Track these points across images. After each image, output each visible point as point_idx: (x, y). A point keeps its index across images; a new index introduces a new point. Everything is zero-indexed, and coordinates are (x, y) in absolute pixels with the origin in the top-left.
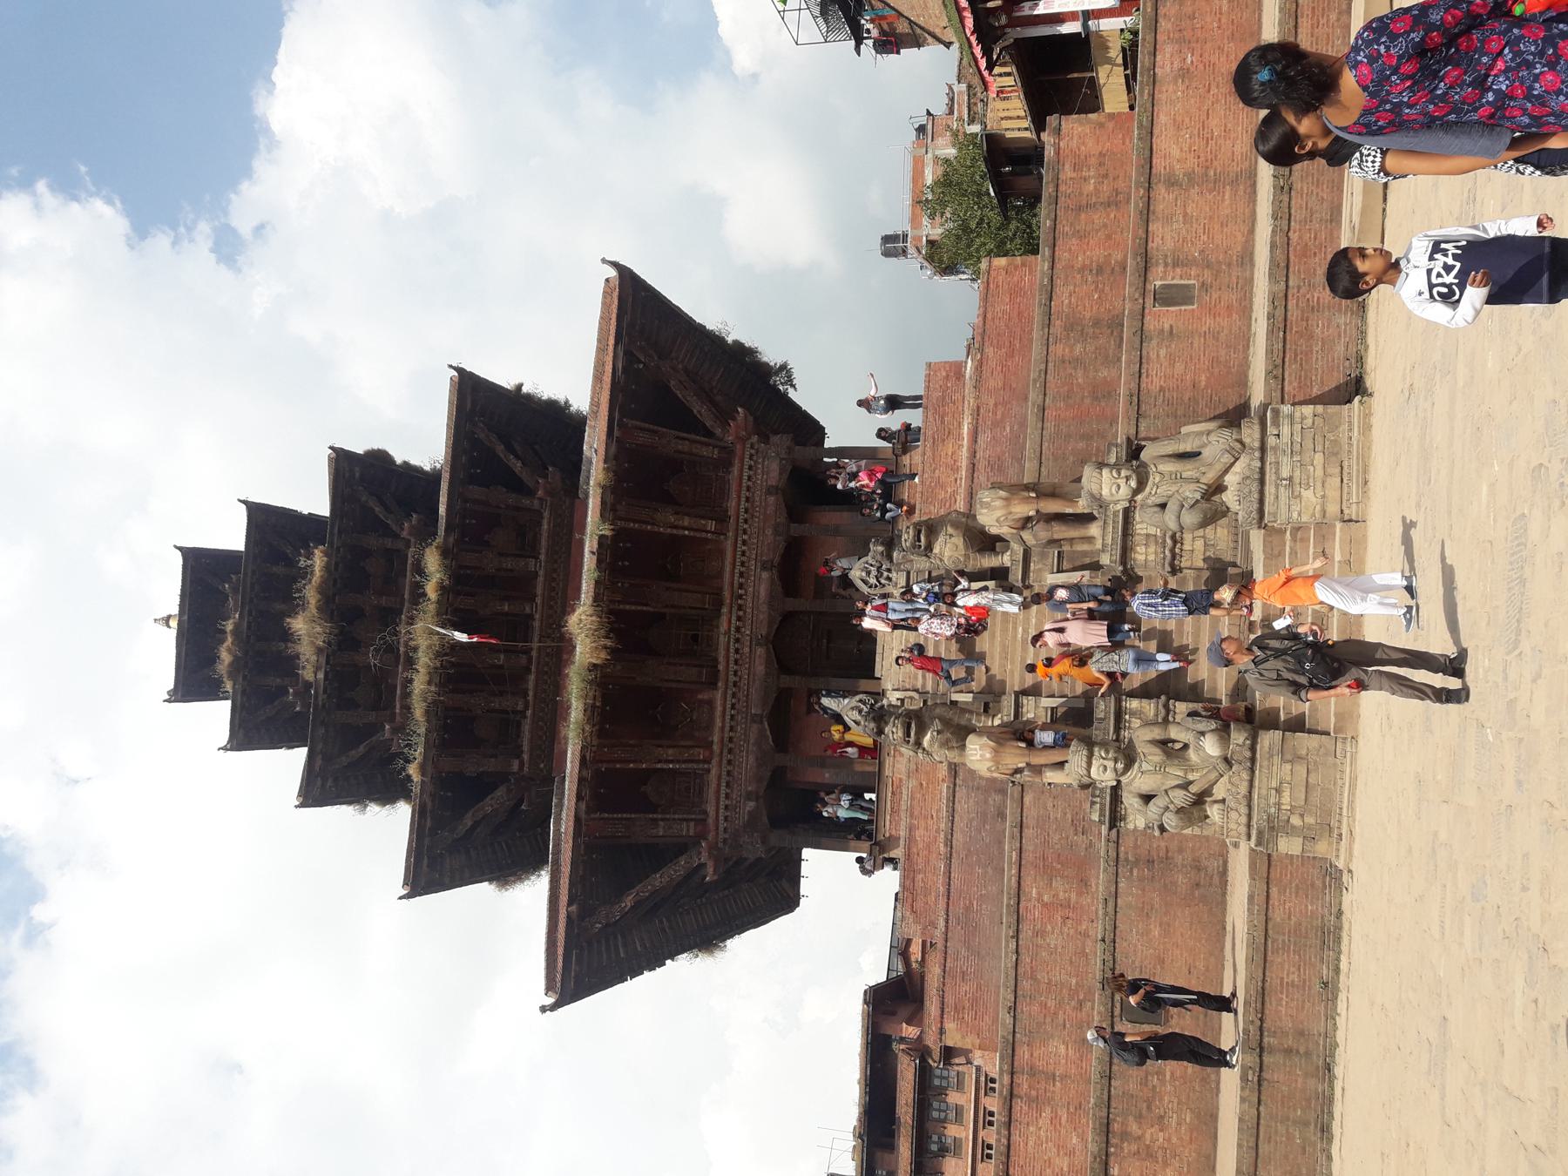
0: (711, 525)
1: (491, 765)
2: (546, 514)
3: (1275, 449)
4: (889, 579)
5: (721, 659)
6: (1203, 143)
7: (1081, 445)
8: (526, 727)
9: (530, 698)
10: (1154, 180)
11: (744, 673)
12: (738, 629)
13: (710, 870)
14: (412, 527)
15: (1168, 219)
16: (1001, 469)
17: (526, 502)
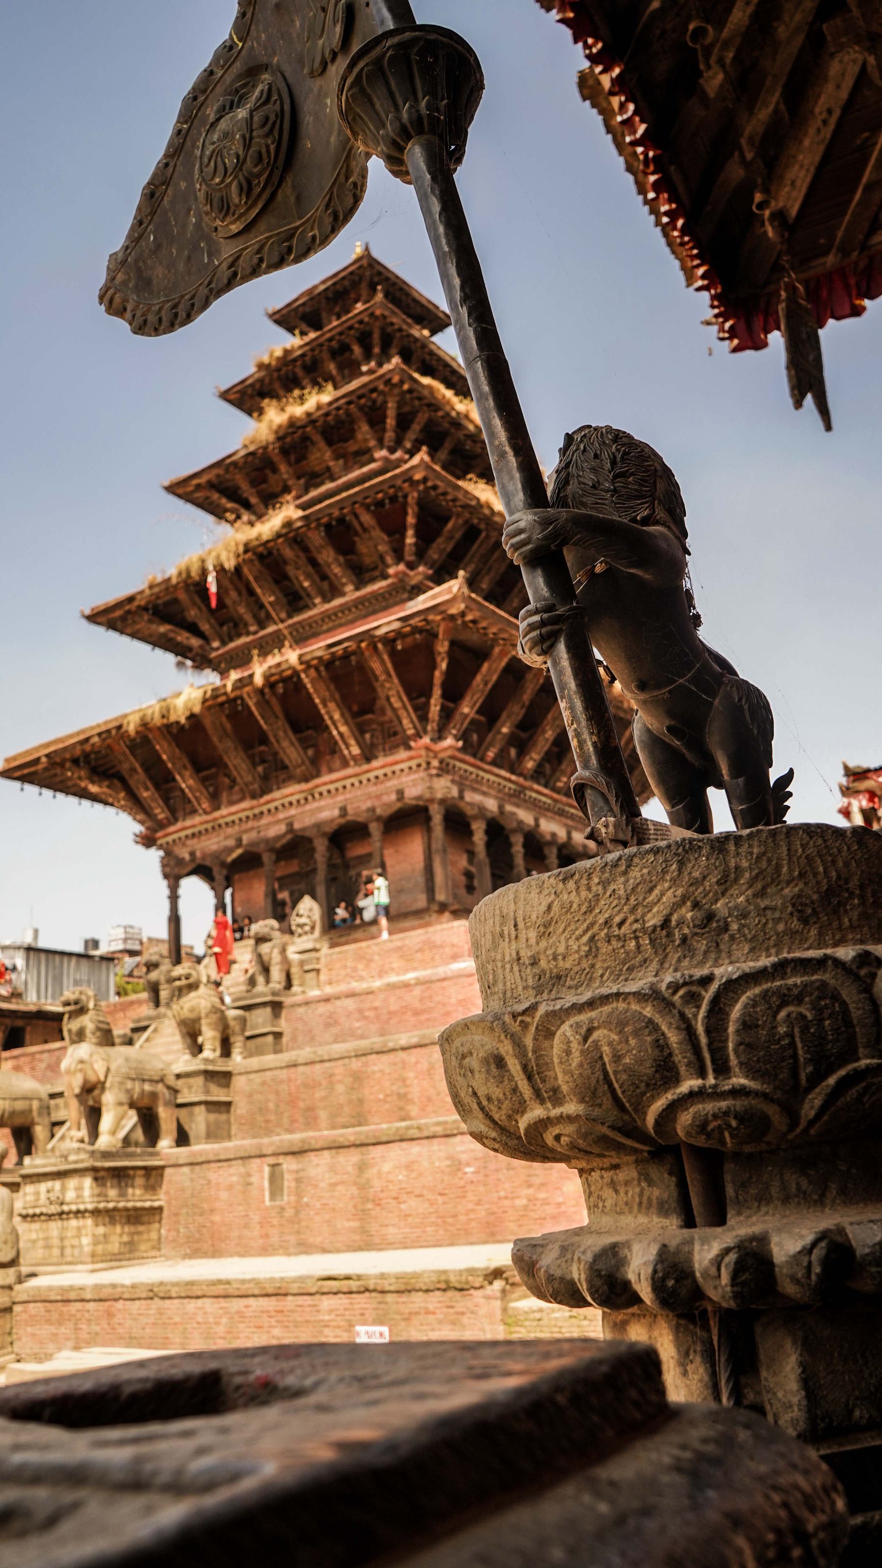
0: (356, 750)
1: (205, 627)
6: (394, 1194)
7: (271, 1105)
9: (262, 633)
10: (363, 1149)
11: (264, 821)
12: (291, 804)
15: (332, 1169)
16: (328, 1025)
17: (389, 560)
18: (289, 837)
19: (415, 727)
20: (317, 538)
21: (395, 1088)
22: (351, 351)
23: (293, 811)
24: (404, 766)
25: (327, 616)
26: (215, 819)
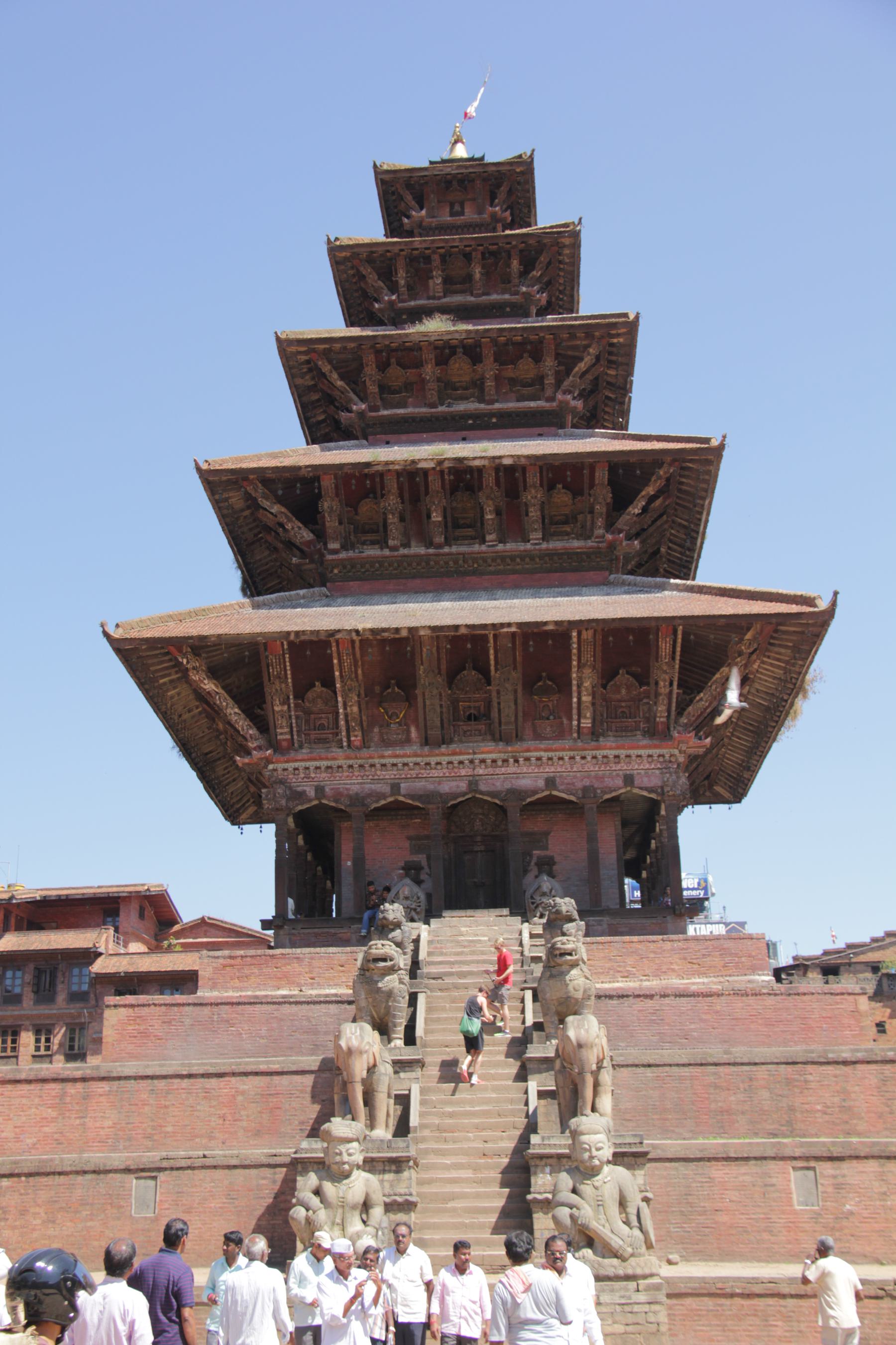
0: (586, 723)
1: (331, 523)
2: (590, 543)
3: (627, 1290)
4: (542, 916)
5: (453, 746)
8: (372, 552)
9: (403, 551)
12: (483, 761)
13: (246, 760)
14: (568, 403)
18: (469, 796)
19: (668, 717)
20: (533, 478)
21: (836, 1100)
22: (509, 266)
25: (502, 558)
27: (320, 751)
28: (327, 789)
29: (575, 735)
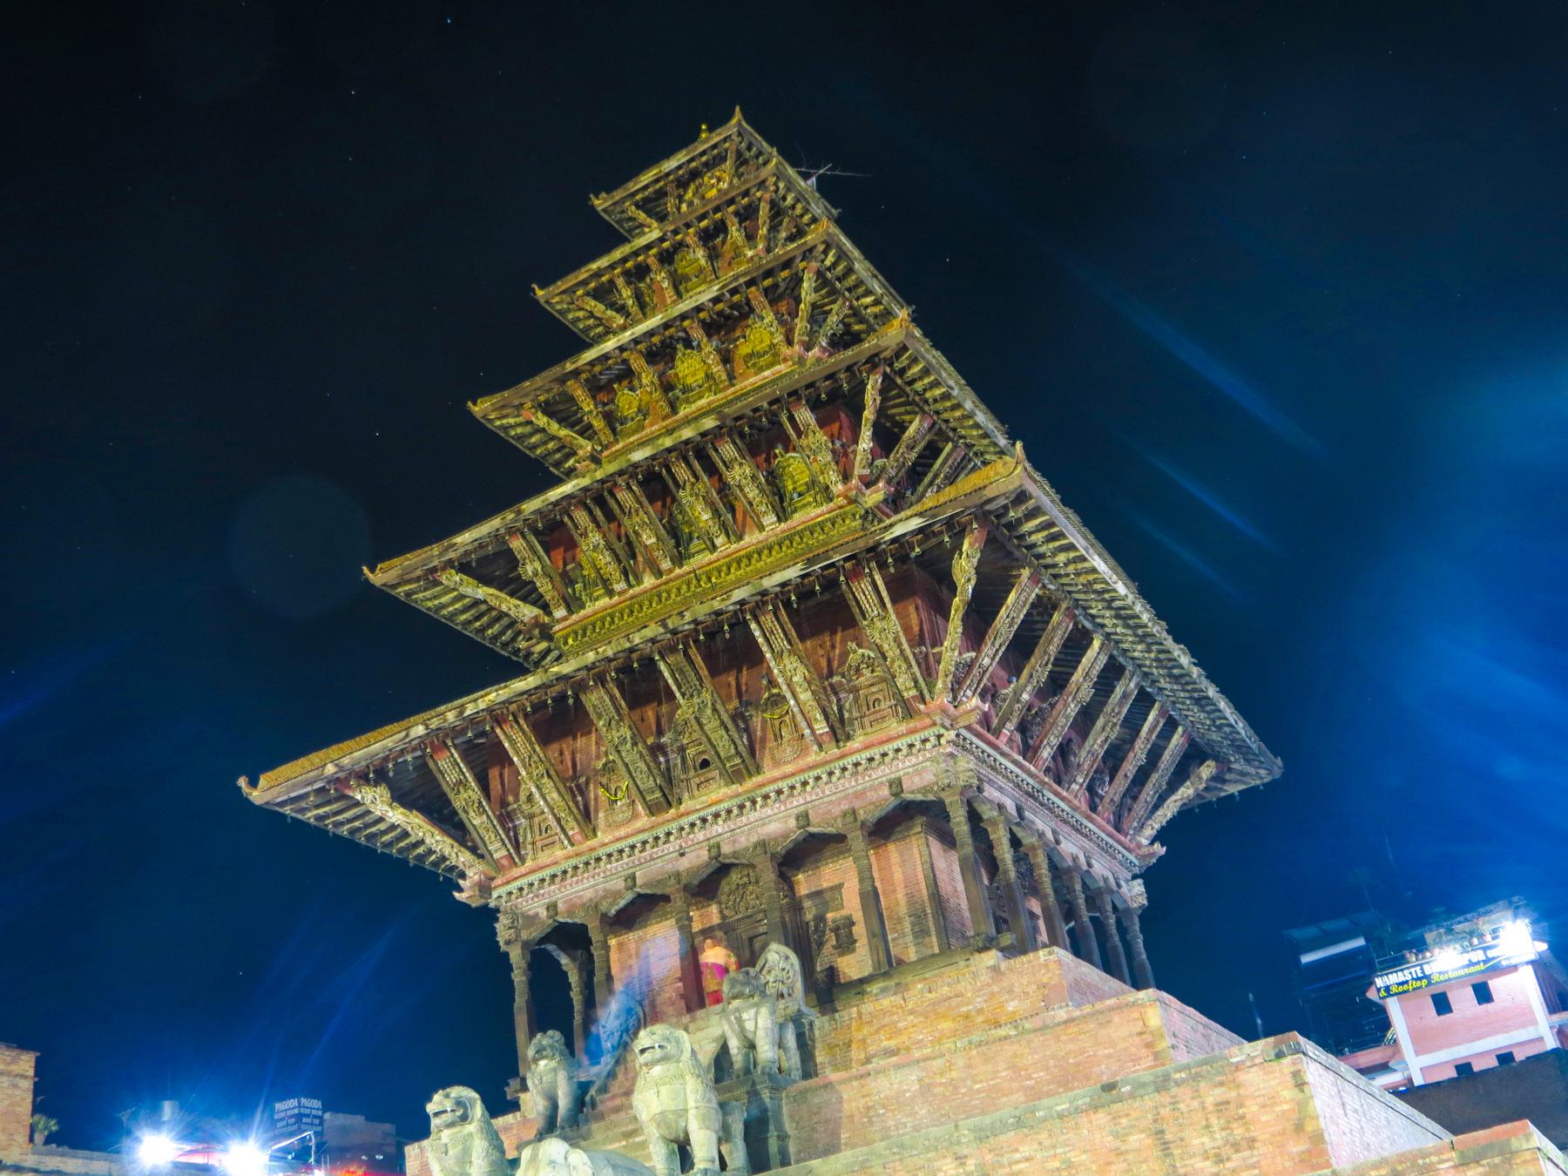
0: (822, 727)
1: (544, 587)
12: (717, 815)
23: (719, 828)
24: (902, 743)
26: (592, 849)
27: (544, 857)
28: (560, 905)
29: (815, 748)
